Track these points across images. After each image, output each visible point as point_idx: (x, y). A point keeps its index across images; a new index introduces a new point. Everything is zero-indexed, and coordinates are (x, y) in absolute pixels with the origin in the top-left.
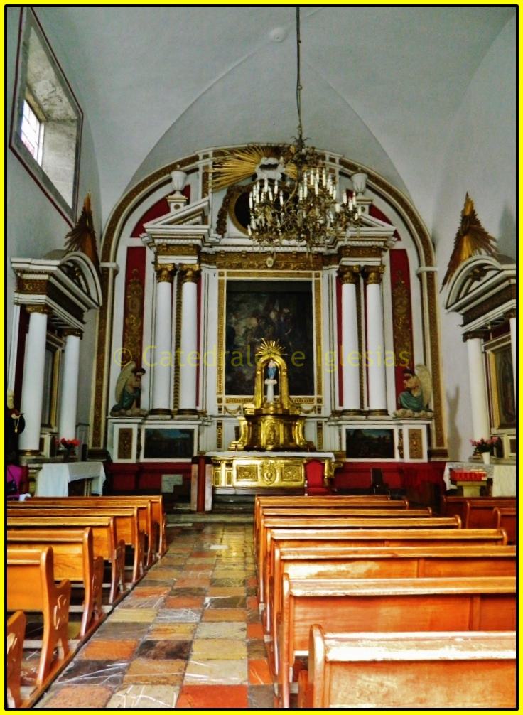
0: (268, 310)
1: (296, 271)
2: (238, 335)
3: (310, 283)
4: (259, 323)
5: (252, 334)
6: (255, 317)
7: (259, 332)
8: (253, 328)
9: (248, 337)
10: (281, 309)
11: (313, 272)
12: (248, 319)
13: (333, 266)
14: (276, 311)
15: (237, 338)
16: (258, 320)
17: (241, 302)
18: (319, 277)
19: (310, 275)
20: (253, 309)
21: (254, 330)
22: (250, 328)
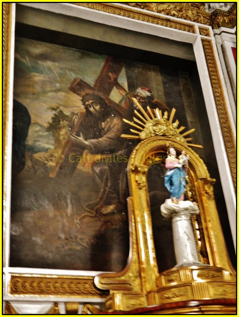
0: (106, 84)
1: (162, 15)
2: (36, 123)
3: (189, 47)
4: (87, 108)
5: (72, 126)
6: (79, 94)
7: (91, 124)
8: (73, 114)
9: (63, 132)
10: (132, 87)
11: (197, 25)
12: (62, 94)
13: (223, 29)
14: (123, 89)
15: (32, 131)
16: (84, 101)
17: (44, 57)
18: (207, 35)
19: (191, 28)
20: (73, 76)
21: (76, 119)
22: (67, 113)
